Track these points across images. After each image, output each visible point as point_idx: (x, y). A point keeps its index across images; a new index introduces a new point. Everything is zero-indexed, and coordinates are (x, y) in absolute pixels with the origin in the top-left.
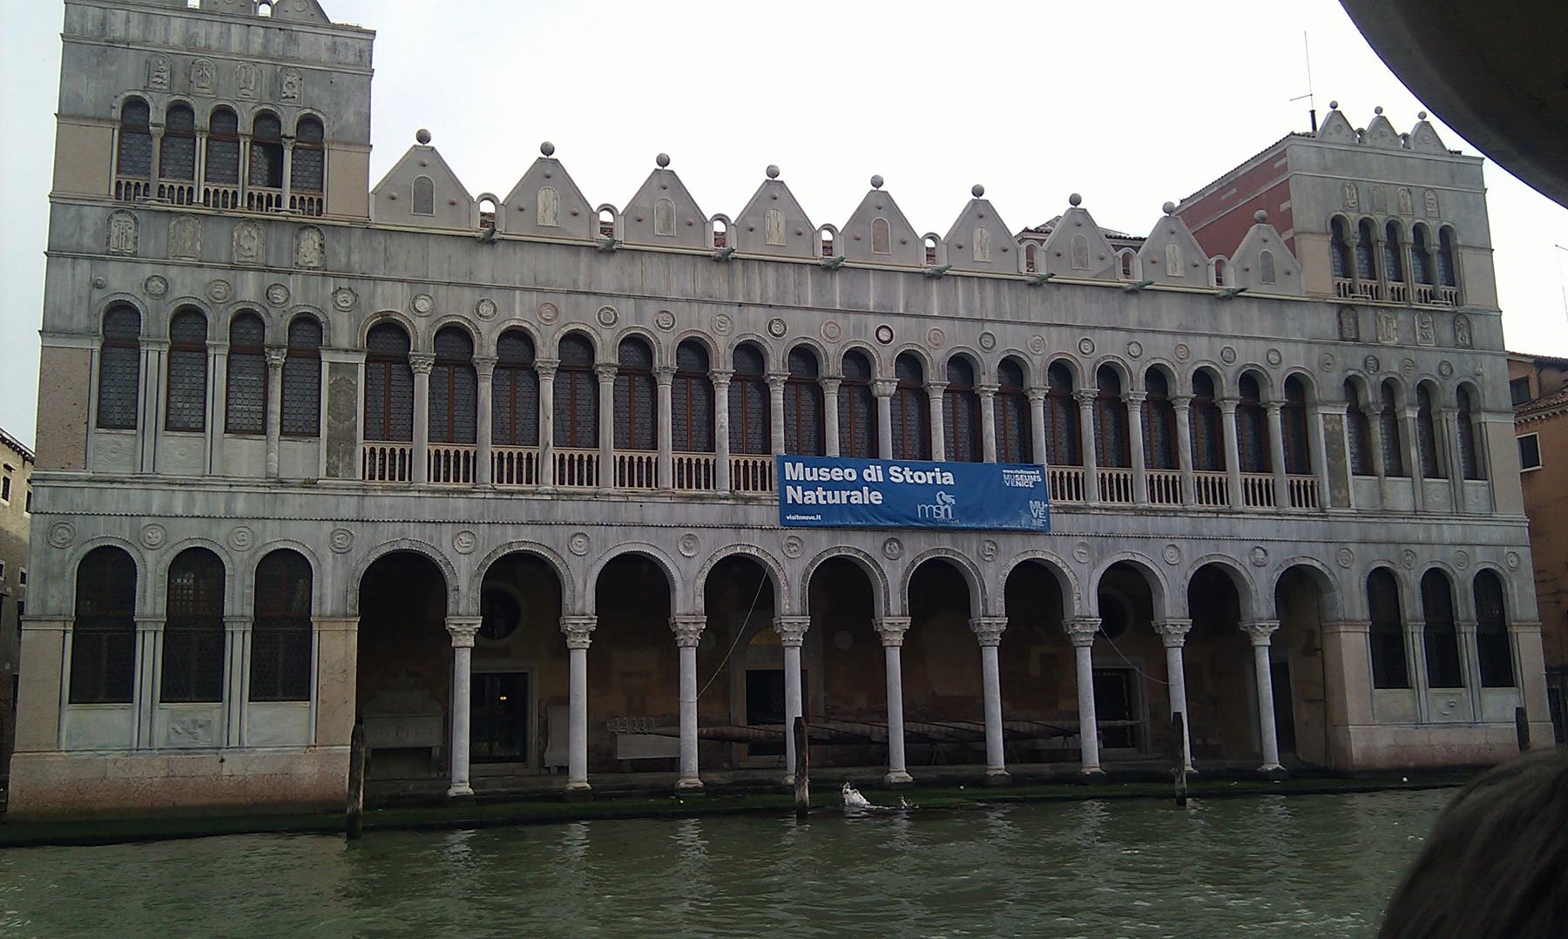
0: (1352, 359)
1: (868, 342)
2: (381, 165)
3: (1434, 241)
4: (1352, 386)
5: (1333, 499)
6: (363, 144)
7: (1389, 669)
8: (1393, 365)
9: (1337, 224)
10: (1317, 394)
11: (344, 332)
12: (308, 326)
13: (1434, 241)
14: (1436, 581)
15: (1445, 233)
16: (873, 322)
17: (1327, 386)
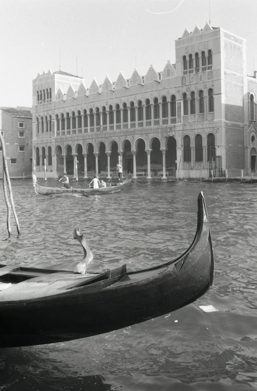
0: (184, 90)
1: (105, 105)
2: (56, 92)
3: (207, 54)
4: (185, 95)
5: (178, 121)
6: (54, 91)
7: (187, 158)
8: (193, 88)
9: (184, 57)
10: (177, 99)
11: (54, 117)
12: (51, 116)
13: (207, 54)
14: (199, 137)
15: (210, 51)
16: (105, 101)
17: (179, 97)
